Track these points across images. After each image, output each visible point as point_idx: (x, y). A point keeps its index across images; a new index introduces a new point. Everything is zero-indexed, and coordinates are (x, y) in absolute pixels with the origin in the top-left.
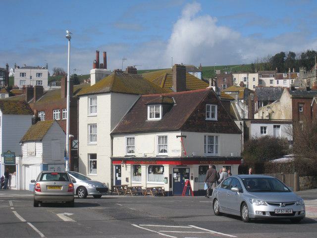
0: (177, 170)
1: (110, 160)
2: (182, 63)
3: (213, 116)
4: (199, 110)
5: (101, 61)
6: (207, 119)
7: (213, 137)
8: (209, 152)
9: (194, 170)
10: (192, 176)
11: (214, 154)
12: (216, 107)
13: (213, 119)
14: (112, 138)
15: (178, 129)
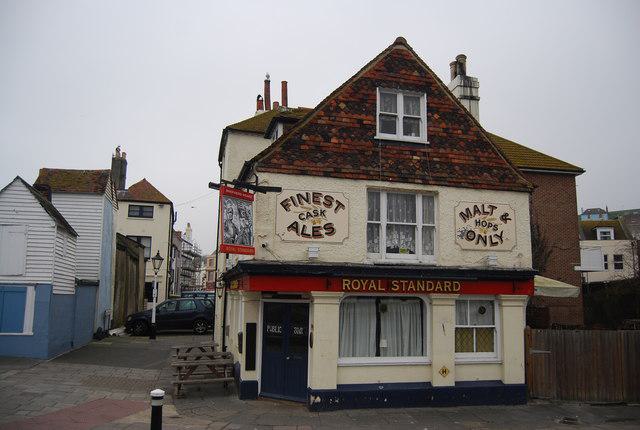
3: (411, 126)
4: (342, 106)
5: (276, 96)
6: (380, 136)
11: (418, 258)
12: (424, 102)
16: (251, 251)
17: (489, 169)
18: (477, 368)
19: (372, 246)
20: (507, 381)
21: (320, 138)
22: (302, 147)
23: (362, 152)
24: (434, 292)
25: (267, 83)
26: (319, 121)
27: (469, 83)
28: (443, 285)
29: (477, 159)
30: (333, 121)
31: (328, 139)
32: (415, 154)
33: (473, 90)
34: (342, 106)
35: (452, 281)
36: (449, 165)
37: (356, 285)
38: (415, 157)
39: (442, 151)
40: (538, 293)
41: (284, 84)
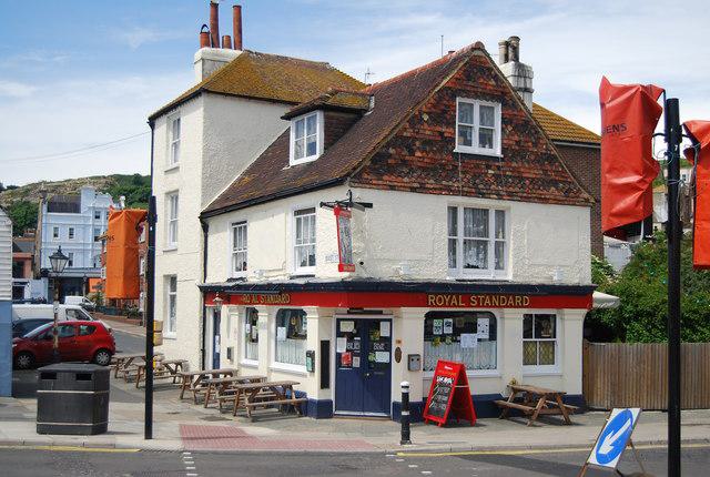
0: (348, 327)
1: (198, 294)
3: (486, 139)
4: (426, 117)
5: (226, 29)
6: (459, 148)
7: (486, 212)
8: (469, 266)
9: (407, 327)
10: (398, 350)
11: (488, 275)
13: (486, 151)
14: (205, 228)
15: (336, 175)
17: (555, 183)
19: (453, 264)
21: (405, 152)
24: (507, 307)
26: (405, 134)
27: (523, 72)
29: (545, 171)
31: (412, 153)
32: (488, 167)
33: (528, 80)
34: (426, 117)
36: (521, 179)
37: (440, 299)
38: (490, 172)
39: (514, 164)
40: (595, 305)
41: (238, 8)
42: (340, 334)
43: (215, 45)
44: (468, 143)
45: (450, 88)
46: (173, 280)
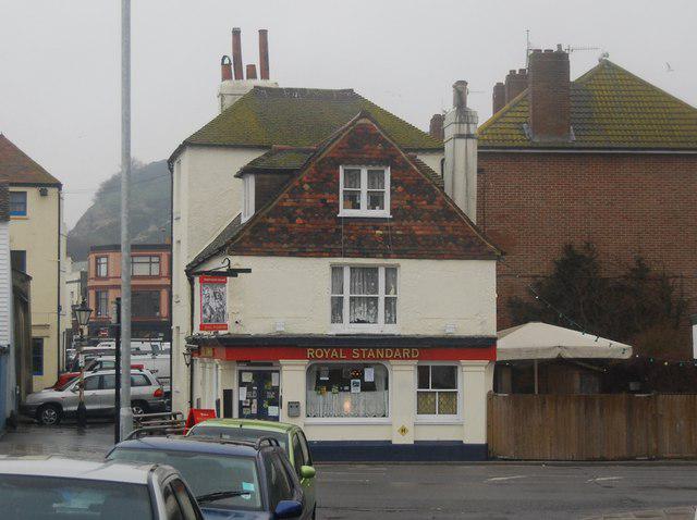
0: (247, 378)
2: (559, 46)
4: (307, 187)
5: (250, 56)
6: (344, 212)
7: (375, 270)
9: (292, 379)
11: (379, 328)
13: (377, 213)
16: (225, 327)
18: (437, 429)
20: (467, 441)
22: (270, 229)
23: (325, 231)
24: (393, 358)
25: (236, 33)
26: (285, 204)
28: (401, 352)
29: (442, 228)
30: (298, 202)
31: (292, 221)
34: (307, 187)
35: (410, 348)
37: (319, 353)
41: (263, 34)
42: (242, 384)
43: (239, 76)
44: (357, 206)
45: (332, 158)
46: (178, 328)
